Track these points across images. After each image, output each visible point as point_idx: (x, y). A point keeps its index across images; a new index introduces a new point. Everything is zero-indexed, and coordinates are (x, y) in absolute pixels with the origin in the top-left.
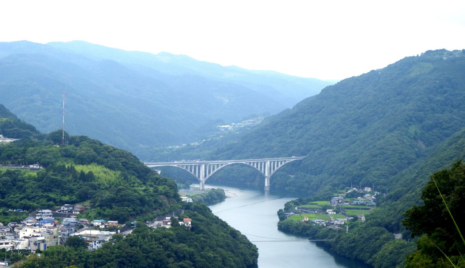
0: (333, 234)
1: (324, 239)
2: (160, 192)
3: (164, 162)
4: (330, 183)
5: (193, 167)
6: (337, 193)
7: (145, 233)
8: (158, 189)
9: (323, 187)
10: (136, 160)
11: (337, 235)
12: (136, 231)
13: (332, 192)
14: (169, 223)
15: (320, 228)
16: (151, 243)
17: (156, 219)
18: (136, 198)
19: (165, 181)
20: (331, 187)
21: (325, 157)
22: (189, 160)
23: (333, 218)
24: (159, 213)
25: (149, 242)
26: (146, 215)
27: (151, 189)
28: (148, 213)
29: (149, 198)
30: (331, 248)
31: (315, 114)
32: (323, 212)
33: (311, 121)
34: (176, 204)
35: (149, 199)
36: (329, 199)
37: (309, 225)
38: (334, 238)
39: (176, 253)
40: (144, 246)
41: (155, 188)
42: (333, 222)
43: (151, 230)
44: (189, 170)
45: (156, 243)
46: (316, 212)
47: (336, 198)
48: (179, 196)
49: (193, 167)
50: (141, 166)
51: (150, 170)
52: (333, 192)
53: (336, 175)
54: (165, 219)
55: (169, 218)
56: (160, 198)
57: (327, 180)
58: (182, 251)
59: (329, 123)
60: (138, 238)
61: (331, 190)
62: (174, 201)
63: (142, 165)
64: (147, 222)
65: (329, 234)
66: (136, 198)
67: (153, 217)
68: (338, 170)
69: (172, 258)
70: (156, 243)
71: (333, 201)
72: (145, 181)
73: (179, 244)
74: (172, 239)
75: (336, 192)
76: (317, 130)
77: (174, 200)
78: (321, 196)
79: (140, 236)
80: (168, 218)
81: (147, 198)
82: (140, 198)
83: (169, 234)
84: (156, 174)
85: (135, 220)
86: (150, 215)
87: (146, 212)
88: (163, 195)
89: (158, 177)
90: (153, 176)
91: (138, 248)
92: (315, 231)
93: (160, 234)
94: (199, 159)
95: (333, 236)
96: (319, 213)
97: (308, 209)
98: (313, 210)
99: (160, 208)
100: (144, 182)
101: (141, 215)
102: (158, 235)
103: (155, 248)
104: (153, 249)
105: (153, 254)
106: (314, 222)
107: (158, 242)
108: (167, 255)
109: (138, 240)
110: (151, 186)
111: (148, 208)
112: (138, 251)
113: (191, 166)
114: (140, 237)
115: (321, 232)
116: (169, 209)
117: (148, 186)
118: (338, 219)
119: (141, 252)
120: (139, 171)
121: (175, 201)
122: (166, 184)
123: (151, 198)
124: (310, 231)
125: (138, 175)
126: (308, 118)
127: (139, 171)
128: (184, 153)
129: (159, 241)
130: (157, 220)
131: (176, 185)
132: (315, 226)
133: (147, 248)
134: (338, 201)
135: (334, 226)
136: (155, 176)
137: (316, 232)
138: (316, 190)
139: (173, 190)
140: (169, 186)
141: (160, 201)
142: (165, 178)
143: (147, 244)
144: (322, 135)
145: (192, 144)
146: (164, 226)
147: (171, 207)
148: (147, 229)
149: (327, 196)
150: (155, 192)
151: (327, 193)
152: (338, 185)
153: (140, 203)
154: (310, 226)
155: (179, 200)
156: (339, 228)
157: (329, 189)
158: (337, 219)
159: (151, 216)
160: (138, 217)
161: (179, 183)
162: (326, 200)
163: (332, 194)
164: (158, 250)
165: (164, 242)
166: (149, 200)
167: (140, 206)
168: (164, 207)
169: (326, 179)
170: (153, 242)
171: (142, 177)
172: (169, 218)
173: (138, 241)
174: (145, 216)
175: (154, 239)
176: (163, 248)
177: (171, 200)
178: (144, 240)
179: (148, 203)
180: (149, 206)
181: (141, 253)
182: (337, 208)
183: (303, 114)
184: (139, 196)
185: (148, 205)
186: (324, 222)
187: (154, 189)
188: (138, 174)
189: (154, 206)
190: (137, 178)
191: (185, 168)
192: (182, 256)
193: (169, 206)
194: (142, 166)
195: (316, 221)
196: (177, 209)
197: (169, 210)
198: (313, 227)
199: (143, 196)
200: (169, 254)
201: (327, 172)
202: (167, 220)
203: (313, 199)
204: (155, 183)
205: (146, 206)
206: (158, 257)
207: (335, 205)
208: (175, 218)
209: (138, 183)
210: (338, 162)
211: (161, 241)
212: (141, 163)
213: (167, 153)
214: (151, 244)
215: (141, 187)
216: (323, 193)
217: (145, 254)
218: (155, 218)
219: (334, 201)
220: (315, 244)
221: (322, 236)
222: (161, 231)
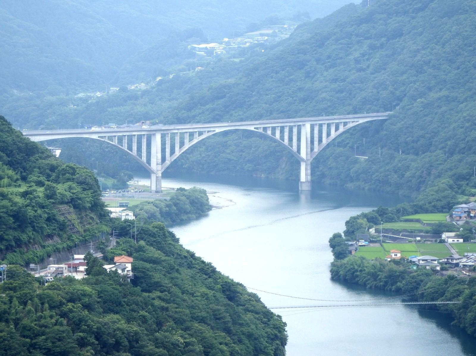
0: (457, 287)
1: (437, 300)
2: (59, 198)
3: (67, 128)
4: (450, 173)
5: (135, 140)
6: (466, 195)
7: (26, 291)
8: (55, 192)
9: (433, 182)
10: (4, 126)
11: (467, 292)
12: (6, 288)
13: (454, 193)
14: (82, 268)
15: (427, 275)
16: (40, 314)
17: (51, 259)
18: (6, 213)
19: (71, 171)
20: (451, 182)
21: (436, 114)
22: (125, 123)
23: (457, 252)
24: (59, 246)
25: (36, 311)
26: (28, 249)
27: (40, 191)
28: (32, 245)
29: (36, 211)
30: (454, 320)
31: (414, 15)
32: (433, 237)
33: (404, 32)
34: (97, 223)
35: (36, 214)
36: (448, 208)
37: (401, 268)
38: (461, 298)
39: (98, 336)
40: (26, 321)
41: (49, 188)
42: (458, 261)
43: (40, 284)
44: (125, 147)
45: (51, 313)
46: (418, 239)
47: (464, 205)
48: (103, 205)
49: (135, 140)
50: (15, 138)
51: (37, 148)
52: (457, 192)
53: (463, 154)
54: (73, 259)
55: (82, 256)
56: (60, 211)
57: (441, 167)
58: (111, 331)
59: (445, 37)
60: (11, 302)
61: (451, 187)
62: (92, 218)
63: (18, 136)
64: (32, 266)
65: (448, 287)
66: (6, 213)
67: (46, 255)
68: (468, 142)
69: (89, 348)
70: (51, 313)
71: (457, 213)
72: (25, 172)
73: (105, 315)
74: (89, 304)
75: (463, 193)
76: (418, 51)
77: (92, 215)
78: (430, 203)
79: (15, 299)
80: (79, 257)
81: (30, 212)
82: (15, 211)
83: (81, 294)
84: (51, 156)
85: (3, 262)
86: (38, 250)
87: (29, 242)
88: (67, 203)
89: (54, 163)
90: (43, 161)
91: (12, 326)
92: (416, 282)
93: (60, 292)
94: (148, 122)
95: (458, 294)
96: (425, 241)
97: (400, 232)
98: (412, 233)
99: (61, 233)
100: (24, 174)
101: (17, 250)
102: (57, 296)
103: (51, 326)
104: (46, 327)
105: (46, 339)
106: (414, 262)
107: (58, 311)
108: (78, 339)
109: (11, 307)
110: (40, 184)
111: (33, 234)
112: (12, 333)
113: (130, 138)
114: (16, 302)
115: (429, 286)
116: (82, 236)
117: (33, 184)
118: (470, 254)
119: (17, 336)
120: (12, 151)
121: (95, 217)
122: (73, 179)
123: (39, 211)
124: (403, 282)
125: (9, 159)
126: (397, 25)
127: (12, 151)
128: (114, 108)
129: (59, 308)
130: (54, 261)
131: (96, 181)
132: (416, 271)
133: (33, 325)
134: (469, 212)
135: (461, 271)
136: (48, 162)
137: (419, 284)
138: (418, 189)
139: (89, 192)
140: (80, 183)
141: (61, 218)
142: (72, 164)
143: (32, 316)
144: (430, 62)
145: (133, 88)
146: (70, 274)
147: (85, 231)
148: (30, 283)
149: (444, 202)
150: (48, 197)
151: (443, 194)
152: (468, 177)
153: (14, 223)
154: (404, 270)
155: (104, 216)
156: (470, 274)
157: (447, 185)
158: (466, 254)
159: (40, 252)
160: (10, 255)
161: (103, 177)
162: (441, 211)
163: (454, 197)
164: (58, 330)
165: (71, 311)
166: (35, 216)
167: (14, 229)
168: (69, 233)
169: (440, 164)
170: (46, 311)
171: (18, 163)
172: (82, 256)
173: (12, 309)
174: (27, 252)
175: (47, 305)
176: (67, 325)
177: (86, 215)
178: (24, 309)
179: (32, 223)
180: (34, 230)
181: (19, 338)
182: (467, 230)
183: (385, 15)
184: (11, 208)
185: (33, 227)
186: (436, 262)
187: (46, 190)
188: (9, 157)
189: (48, 230)
190: (5, 167)
191: (115, 142)
192: (112, 342)
193: (81, 230)
194: (19, 139)
195: (419, 260)
196: (98, 234)
197: (81, 238)
198: (411, 273)
199: (20, 208)
200: (82, 338)
201: (443, 148)
202: (77, 262)
203: (410, 210)
204: (48, 176)
205: (29, 231)
206: (57, 347)
207: (461, 223)
208: (95, 255)
209: (9, 177)
210: (467, 125)
211: (65, 309)
212: (16, 132)
213: (76, 110)
214: (41, 317)
215: (16, 186)
216: (432, 195)
217: (28, 340)
218: (49, 256)
219: (459, 213)
220: (416, 311)
221: (433, 293)
222: (64, 287)
